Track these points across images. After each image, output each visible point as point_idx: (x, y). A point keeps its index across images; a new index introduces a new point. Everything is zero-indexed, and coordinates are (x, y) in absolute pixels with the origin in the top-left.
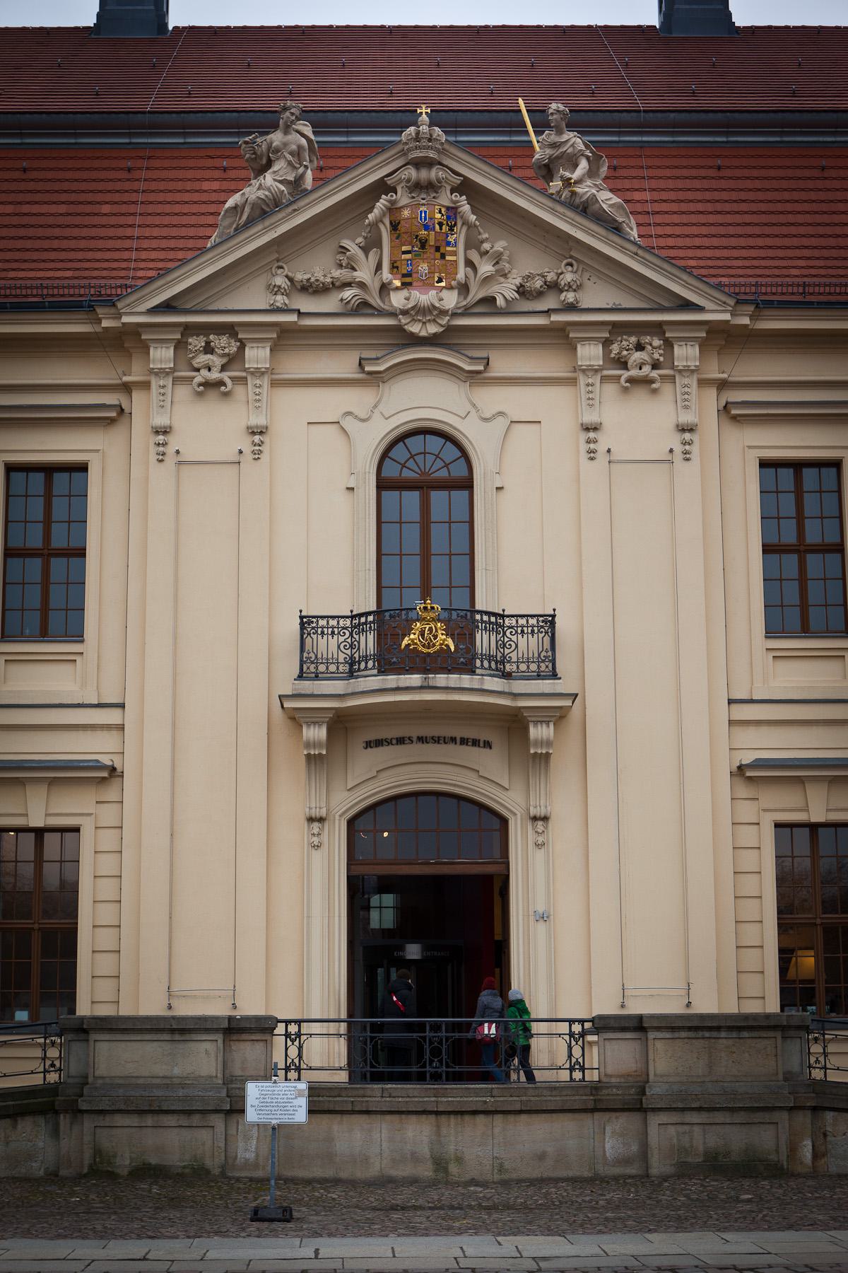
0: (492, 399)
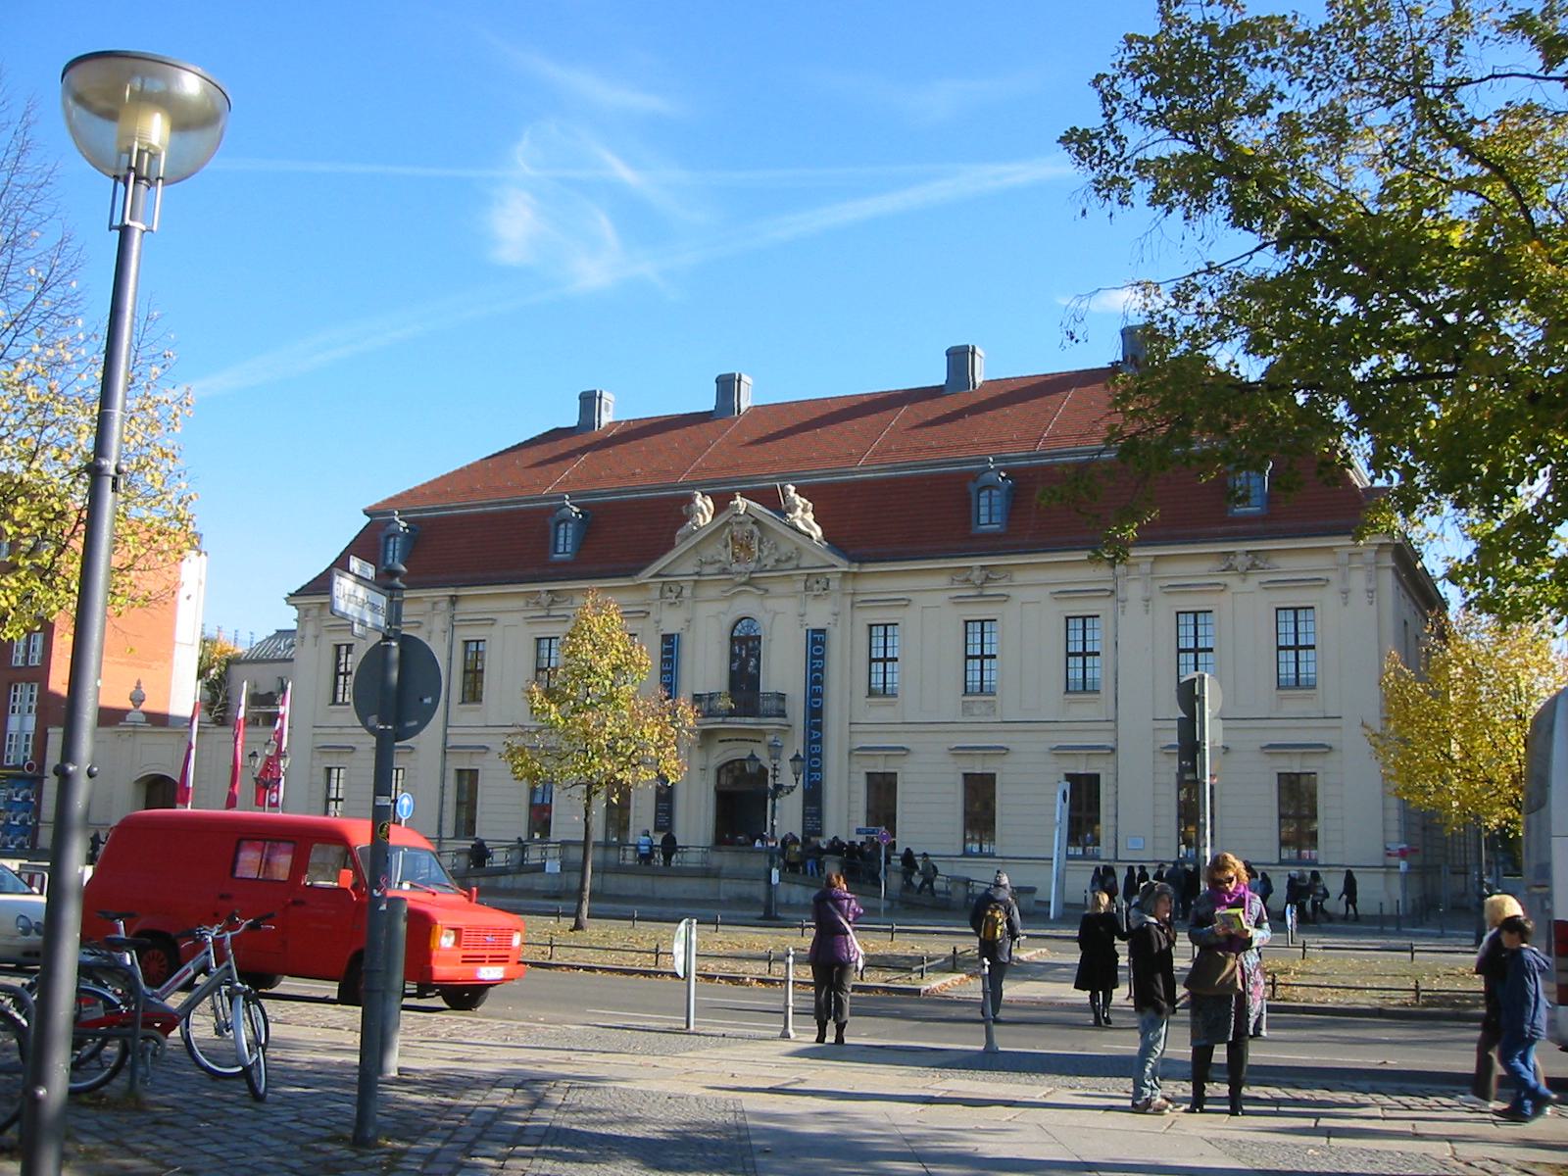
0: (770, 603)
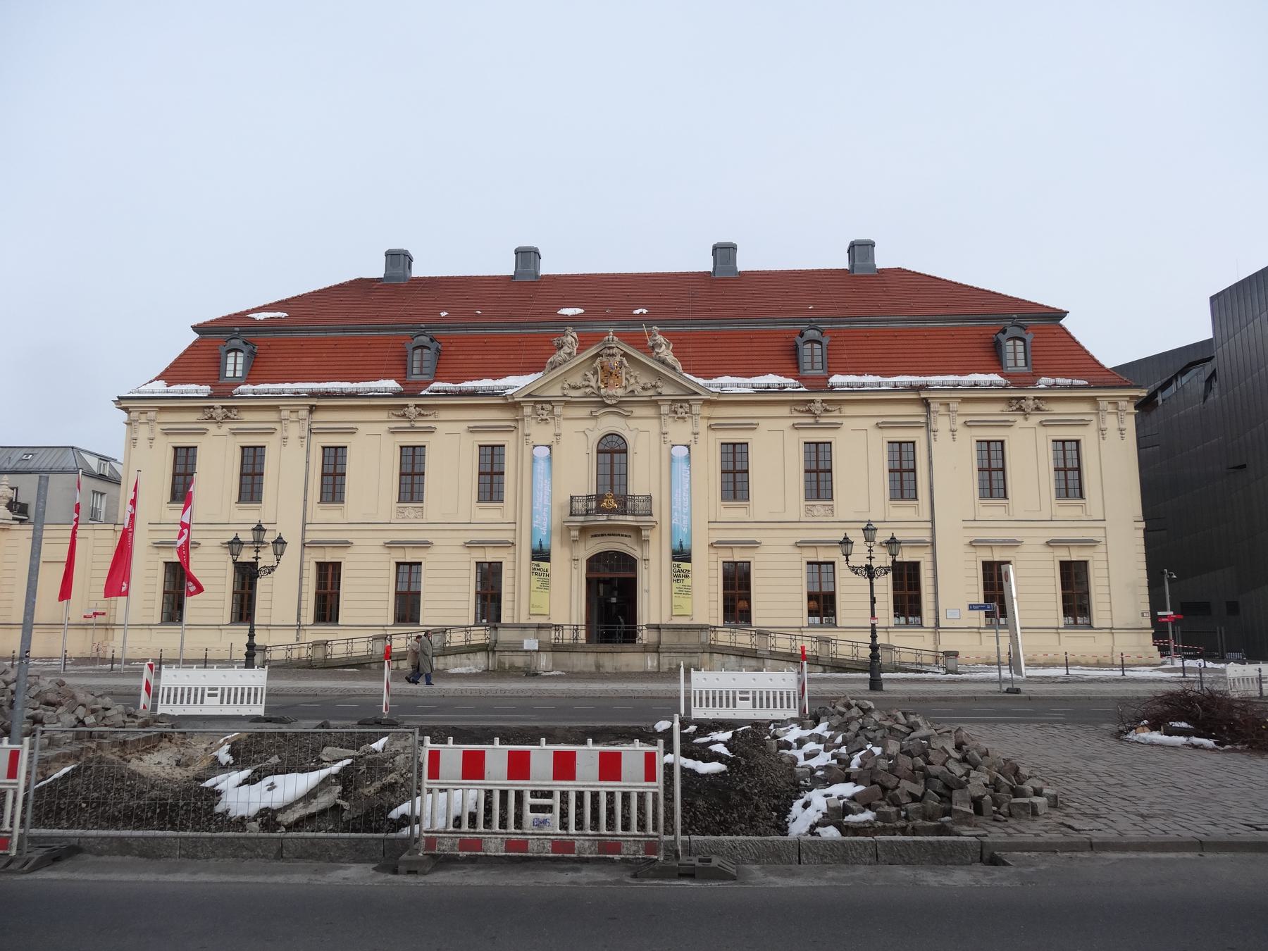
0: (632, 423)
